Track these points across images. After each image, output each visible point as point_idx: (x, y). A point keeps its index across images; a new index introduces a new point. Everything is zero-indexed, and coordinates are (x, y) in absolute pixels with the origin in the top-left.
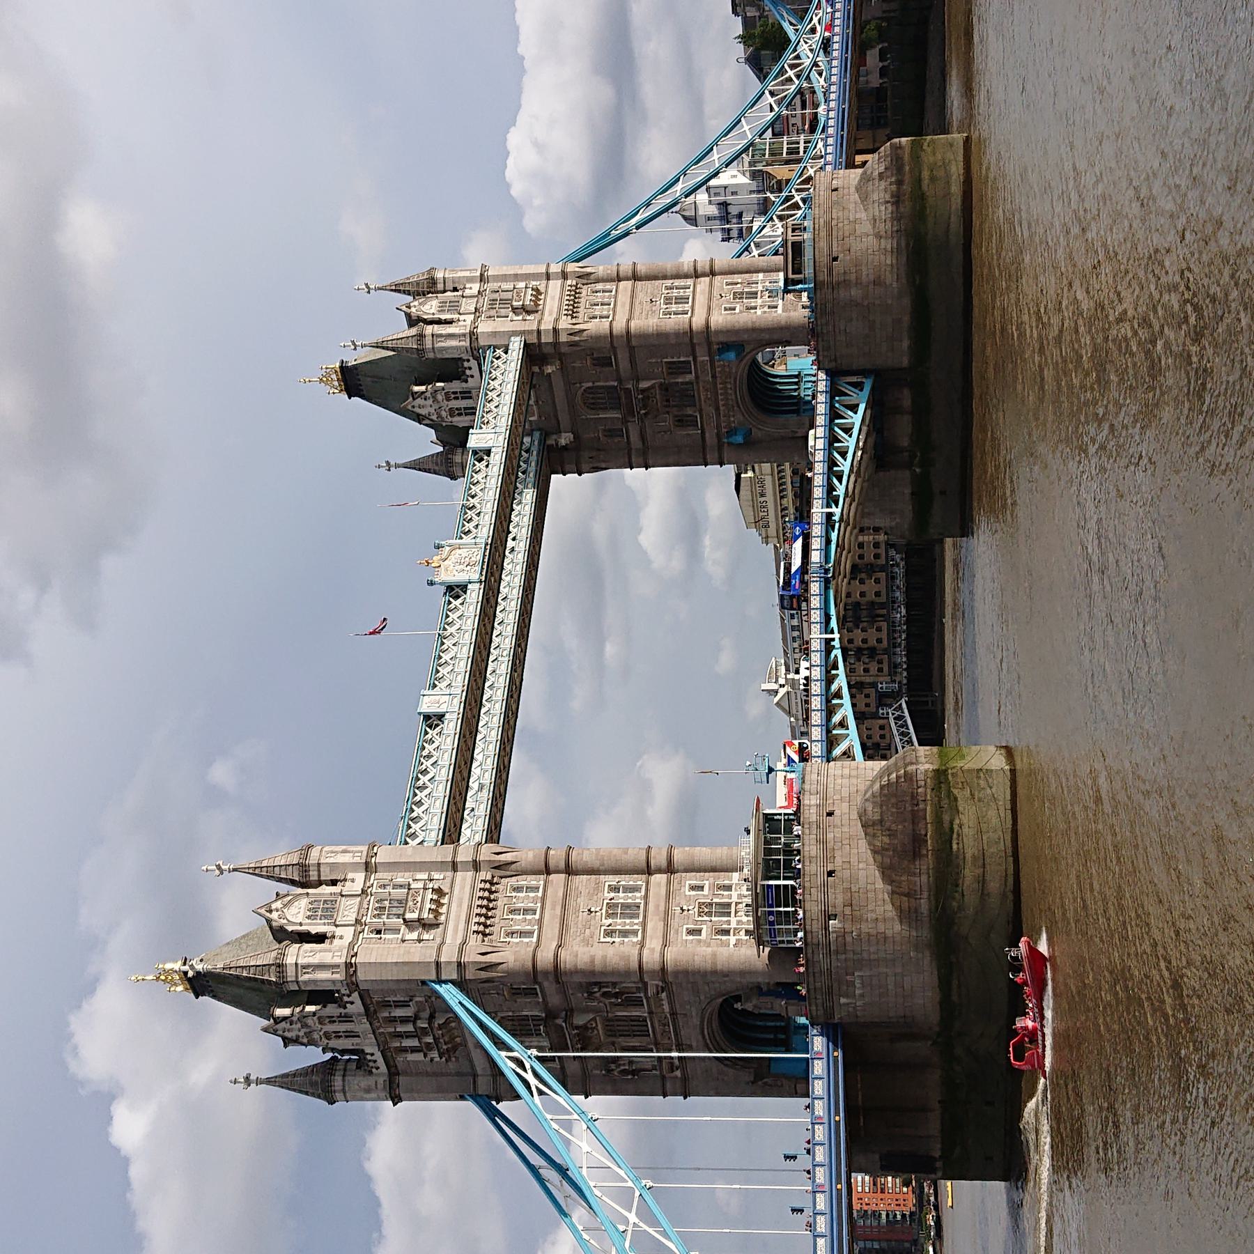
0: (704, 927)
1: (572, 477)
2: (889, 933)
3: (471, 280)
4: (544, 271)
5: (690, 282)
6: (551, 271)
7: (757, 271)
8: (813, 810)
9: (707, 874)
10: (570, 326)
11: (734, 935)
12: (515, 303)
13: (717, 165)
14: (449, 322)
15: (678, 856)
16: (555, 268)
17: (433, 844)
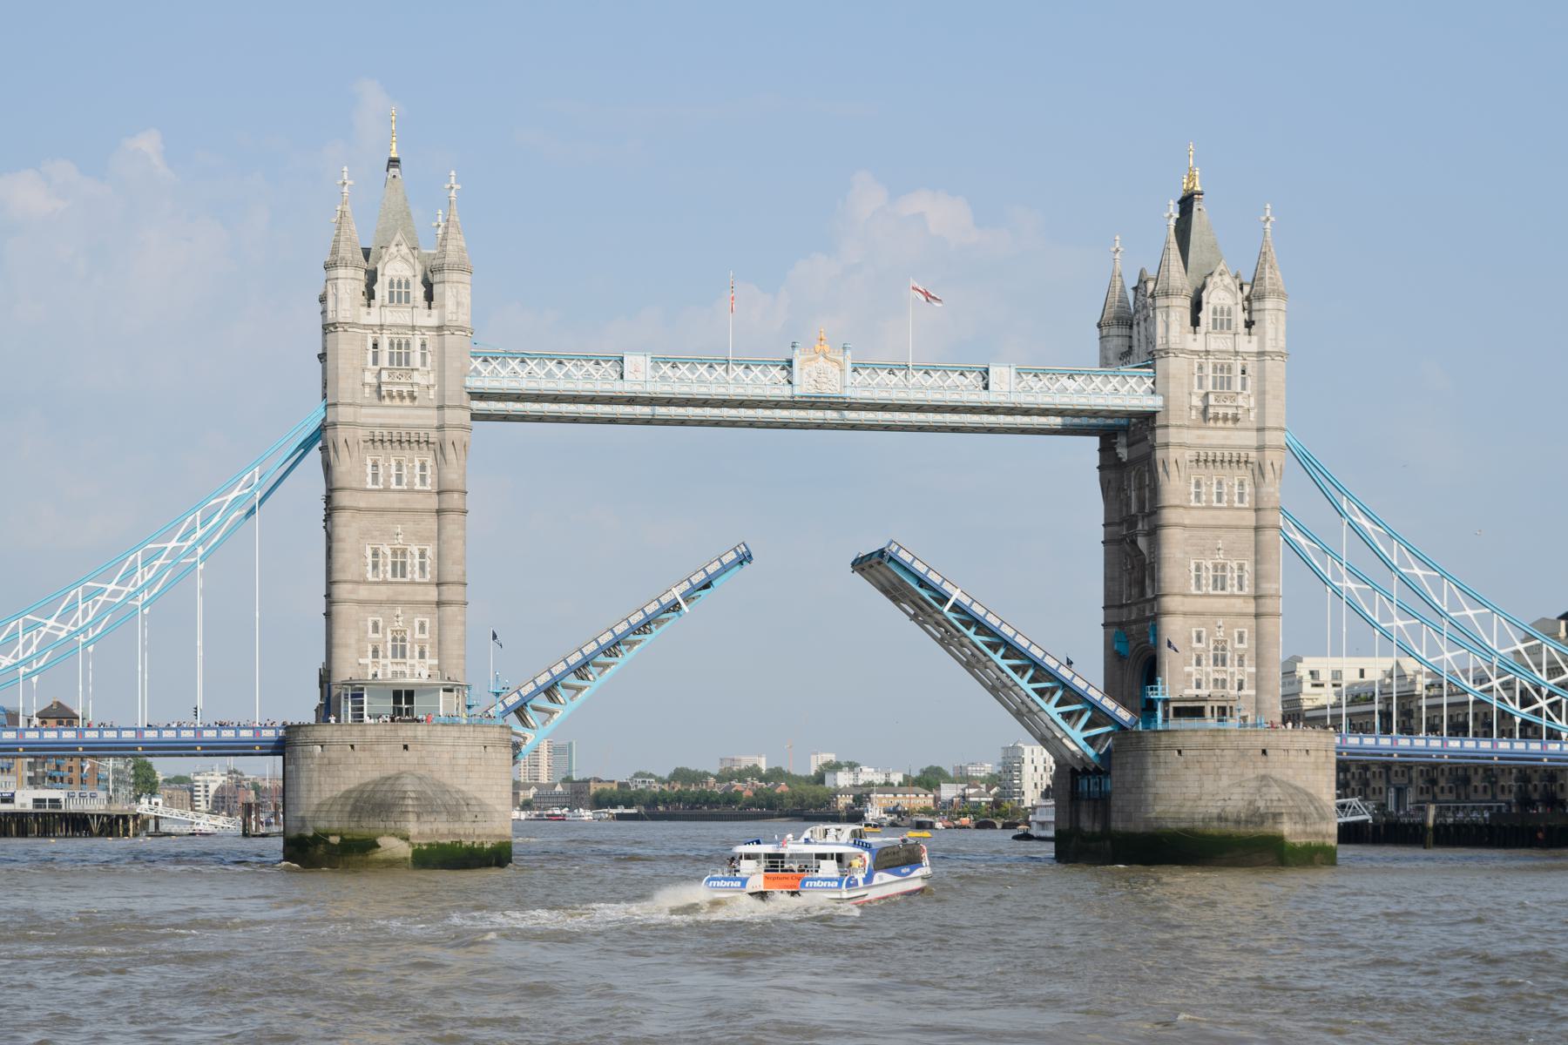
0: (381, 636)
1: (1095, 459)
2: (313, 794)
3: (1262, 341)
4: (1268, 424)
5: (1247, 590)
6: (1267, 433)
7: (1257, 666)
8: (410, 733)
9: (436, 636)
10: (1172, 460)
11: (373, 662)
12: (1212, 398)
13: (1452, 615)
14: (1195, 322)
15: (449, 610)
16: (1271, 438)
17: (468, 384)
